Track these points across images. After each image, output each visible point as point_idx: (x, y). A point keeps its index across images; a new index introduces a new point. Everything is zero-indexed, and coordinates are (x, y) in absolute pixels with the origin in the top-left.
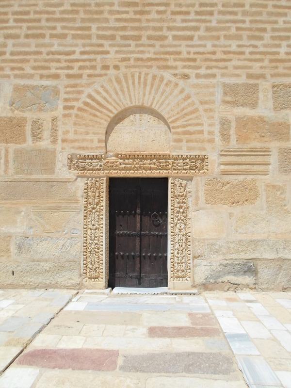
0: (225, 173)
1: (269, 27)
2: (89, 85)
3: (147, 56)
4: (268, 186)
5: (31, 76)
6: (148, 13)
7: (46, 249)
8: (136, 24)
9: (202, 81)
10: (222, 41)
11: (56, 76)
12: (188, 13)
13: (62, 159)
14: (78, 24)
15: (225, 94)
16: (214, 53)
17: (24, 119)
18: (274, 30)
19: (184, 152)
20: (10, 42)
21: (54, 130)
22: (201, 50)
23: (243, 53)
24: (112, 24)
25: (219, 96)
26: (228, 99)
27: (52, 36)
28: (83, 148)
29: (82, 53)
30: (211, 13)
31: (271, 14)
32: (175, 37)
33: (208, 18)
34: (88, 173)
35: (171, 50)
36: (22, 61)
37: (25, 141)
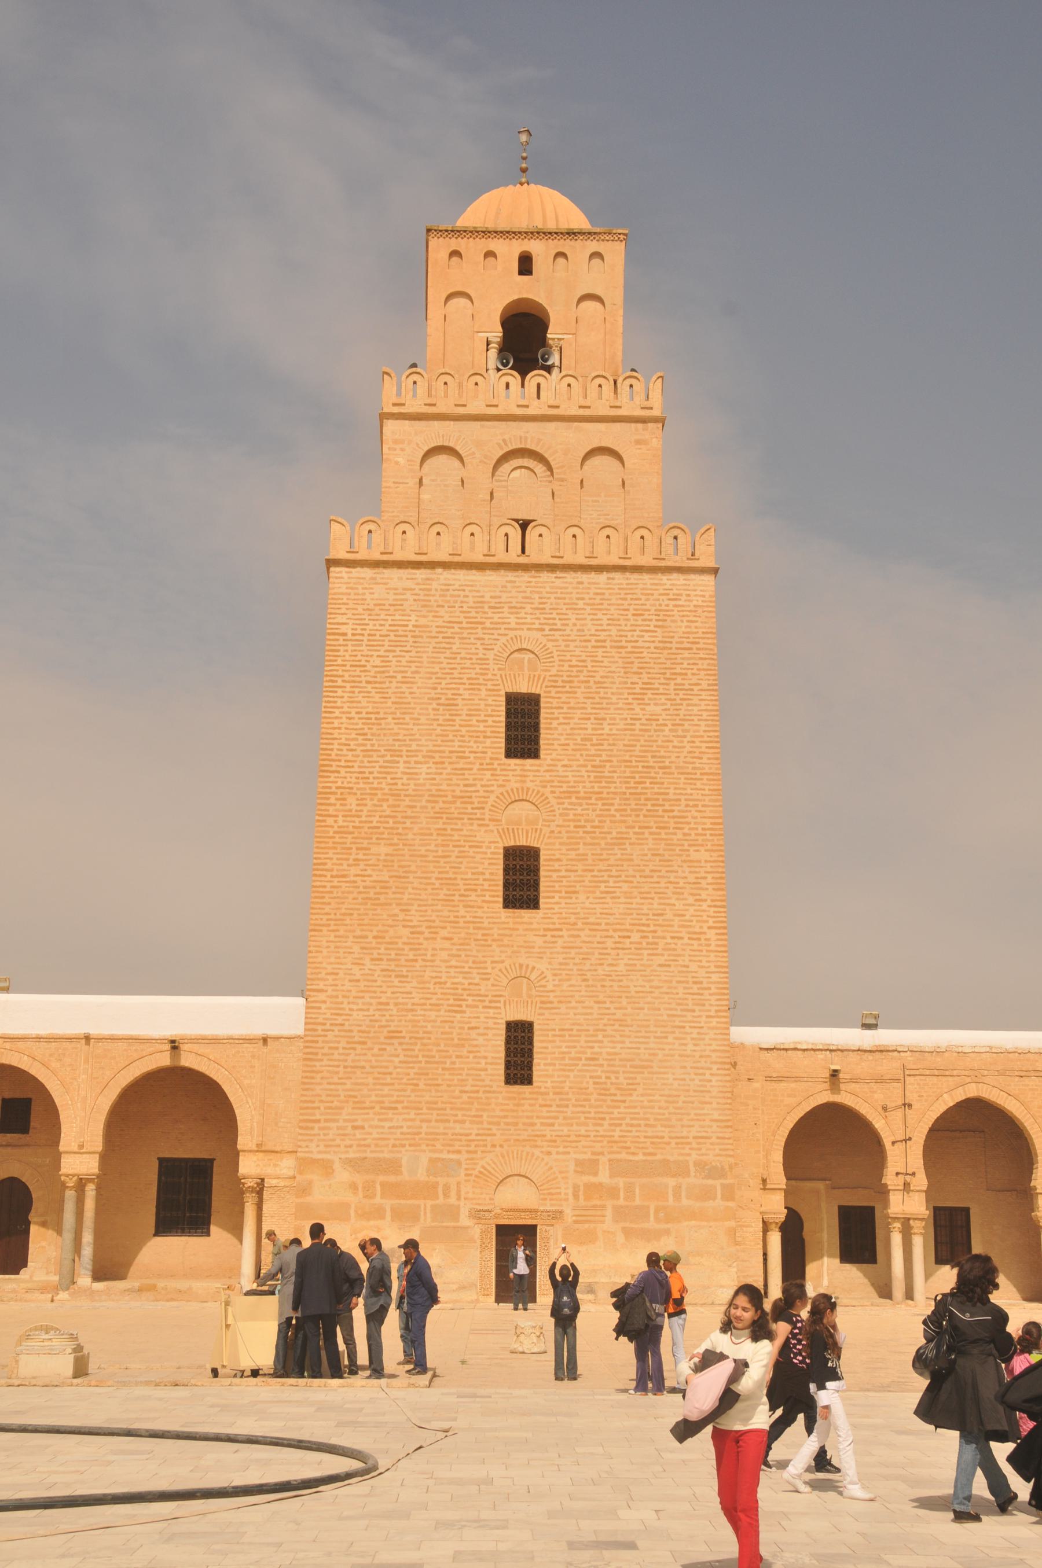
0: (576, 1222)
1: (607, 1116)
2: (482, 1158)
3: (521, 1138)
4: (604, 1231)
5: (441, 1151)
6: (523, 1105)
8: (515, 1114)
9: (560, 1157)
10: (575, 1127)
11: (459, 1152)
12: (551, 1106)
13: (464, 1213)
14: (473, 1113)
15: (576, 1165)
16: (569, 1136)
17: (437, 1183)
18: (611, 1119)
19: (548, 1208)
20: (424, 1125)
21: (459, 1192)
22: (560, 1133)
23: (588, 1136)
25: (572, 1167)
26: (579, 1169)
27: (455, 1122)
28: (479, 1204)
29: (477, 1135)
30: (567, 1106)
31: (609, 1107)
32: (542, 1124)
33: (565, 1109)
34: (483, 1221)
35: (538, 1133)
36: (434, 1140)
37: (438, 1198)
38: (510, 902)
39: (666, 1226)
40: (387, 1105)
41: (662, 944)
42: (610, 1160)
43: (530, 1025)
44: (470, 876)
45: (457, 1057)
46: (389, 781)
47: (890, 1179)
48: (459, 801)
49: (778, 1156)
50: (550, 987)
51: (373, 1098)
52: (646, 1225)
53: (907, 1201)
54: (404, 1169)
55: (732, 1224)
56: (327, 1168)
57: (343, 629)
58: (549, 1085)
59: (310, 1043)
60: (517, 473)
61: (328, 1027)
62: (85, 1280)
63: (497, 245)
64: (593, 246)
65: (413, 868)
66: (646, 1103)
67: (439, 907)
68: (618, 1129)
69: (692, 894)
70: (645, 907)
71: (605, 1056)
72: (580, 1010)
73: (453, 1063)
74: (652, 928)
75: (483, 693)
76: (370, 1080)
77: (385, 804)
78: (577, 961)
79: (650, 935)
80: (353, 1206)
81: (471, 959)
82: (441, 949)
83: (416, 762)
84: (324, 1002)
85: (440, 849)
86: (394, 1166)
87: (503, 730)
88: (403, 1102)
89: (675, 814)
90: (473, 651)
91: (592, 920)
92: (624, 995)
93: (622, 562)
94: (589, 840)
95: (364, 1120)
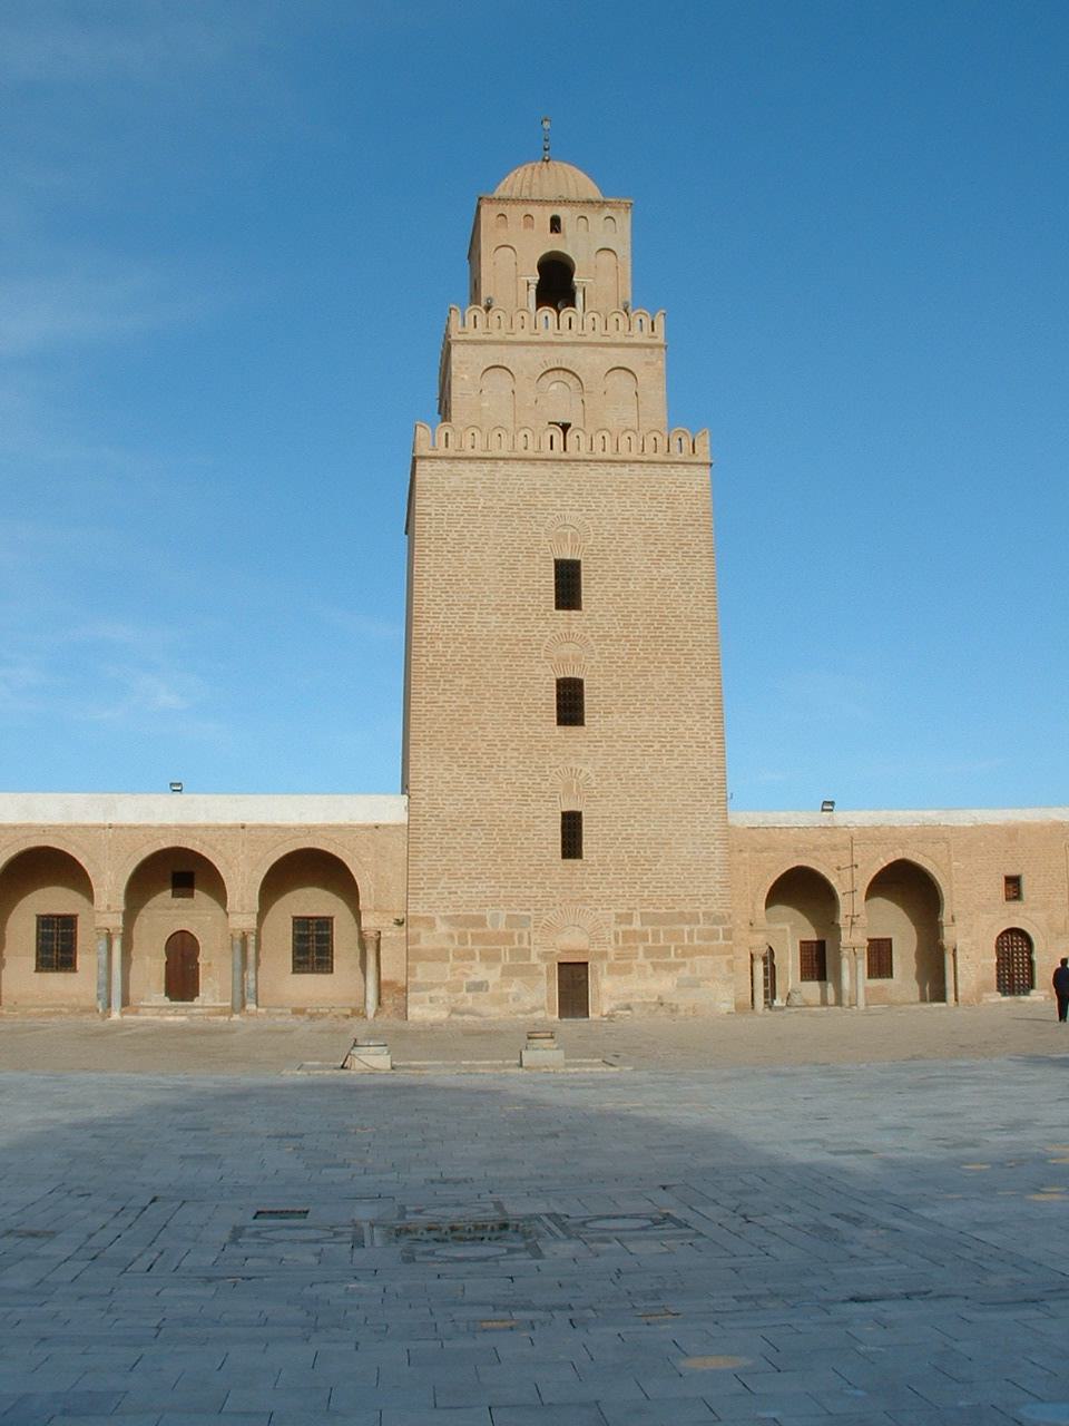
4: (638, 966)
7: (529, 1000)
9: (605, 912)
10: (615, 889)
11: (529, 910)
14: (539, 880)
19: (596, 949)
20: (503, 890)
21: (529, 938)
24: (557, 880)
32: (591, 888)
38: (562, 721)
39: (683, 960)
40: (474, 876)
41: (676, 751)
42: (641, 914)
43: (580, 813)
44: (531, 700)
45: (526, 839)
46: (467, 628)
47: (842, 921)
48: (521, 643)
50: (594, 785)
51: (463, 871)
52: (668, 960)
54: (488, 923)
55: (731, 957)
57: (428, 510)
58: (595, 858)
59: (410, 829)
60: (554, 387)
61: (427, 818)
63: (534, 210)
64: (608, 211)
65: (488, 696)
66: (667, 871)
67: (509, 725)
68: (646, 890)
69: (698, 713)
70: (664, 723)
71: (636, 836)
72: (617, 802)
73: (522, 843)
74: (669, 739)
75: (537, 560)
76: (460, 857)
77: (465, 647)
78: (614, 765)
79: (668, 745)
80: (451, 950)
81: (534, 765)
82: (512, 758)
83: (488, 614)
84: (423, 799)
85: (508, 681)
86: (480, 921)
87: (553, 588)
88: (485, 873)
89: (685, 652)
90: (529, 526)
91: (624, 734)
92: (649, 790)
93: (640, 458)
94: (619, 673)
95: (458, 887)
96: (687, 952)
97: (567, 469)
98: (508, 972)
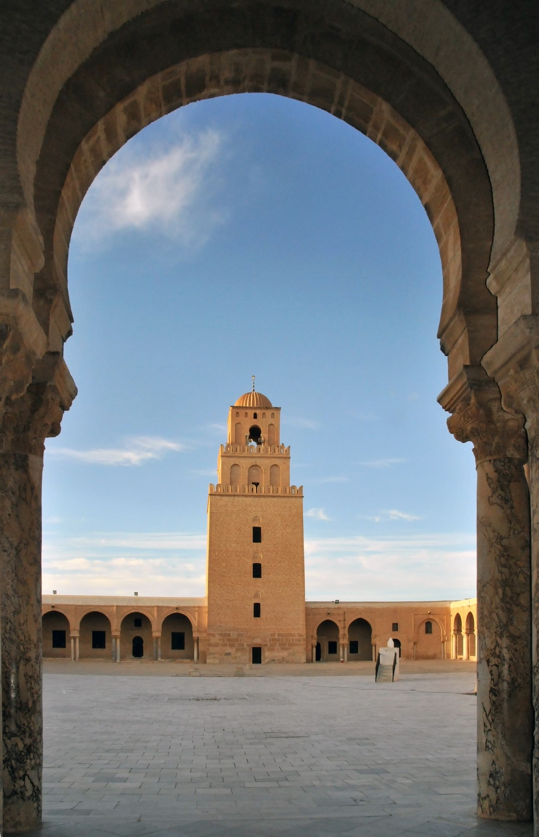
43: (259, 604)
47: (340, 636)
49: (315, 632)
53: (344, 641)
56: (214, 635)
57: (214, 511)
60: (254, 471)
62: (159, 659)
86: (229, 635)
96: (291, 645)
97: (257, 499)
98: (237, 650)
